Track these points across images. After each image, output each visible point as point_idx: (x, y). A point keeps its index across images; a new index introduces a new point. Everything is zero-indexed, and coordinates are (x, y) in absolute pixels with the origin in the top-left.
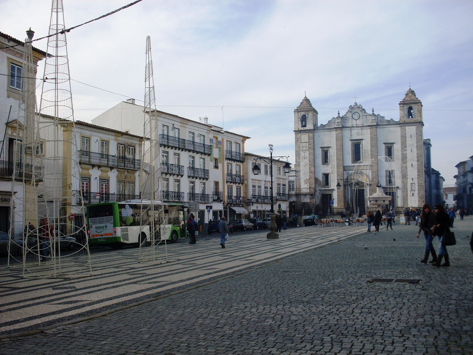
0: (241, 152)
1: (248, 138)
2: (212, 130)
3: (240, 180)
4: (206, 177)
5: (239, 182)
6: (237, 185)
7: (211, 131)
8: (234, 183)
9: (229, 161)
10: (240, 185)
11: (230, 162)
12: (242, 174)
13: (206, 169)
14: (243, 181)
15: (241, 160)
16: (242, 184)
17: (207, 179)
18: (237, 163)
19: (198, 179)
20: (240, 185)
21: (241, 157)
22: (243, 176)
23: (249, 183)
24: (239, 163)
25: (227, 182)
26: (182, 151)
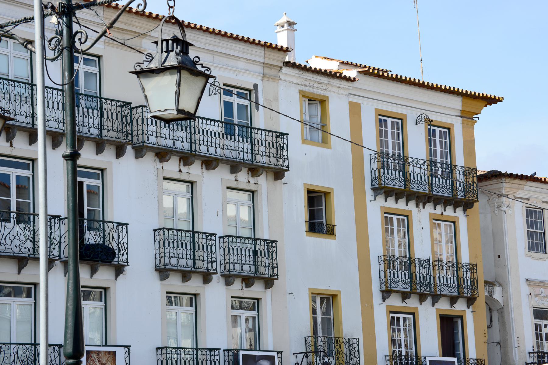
0: (460, 160)
1: (491, 101)
2: (288, 64)
3: (459, 286)
4: (263, 271)
5: (406, 288)
6: (444, 305)
7: (285, 70)
8: (422, 298)
9: (391, 203)
10: (460, 306)
11: (401, 205)
12: (465, 259)
13: (264, 233)
14: (474, 287)
15: (460, 195)
16: (471, 301)
17: (269, 283)
18: (439, 209)
19: (217, 282)
20: (460, 306)
21: (460, 186)
22: (472, 268)
23: (513, 302)
24: (449, 212)
25: (386, 293)
26: (120, 152)
